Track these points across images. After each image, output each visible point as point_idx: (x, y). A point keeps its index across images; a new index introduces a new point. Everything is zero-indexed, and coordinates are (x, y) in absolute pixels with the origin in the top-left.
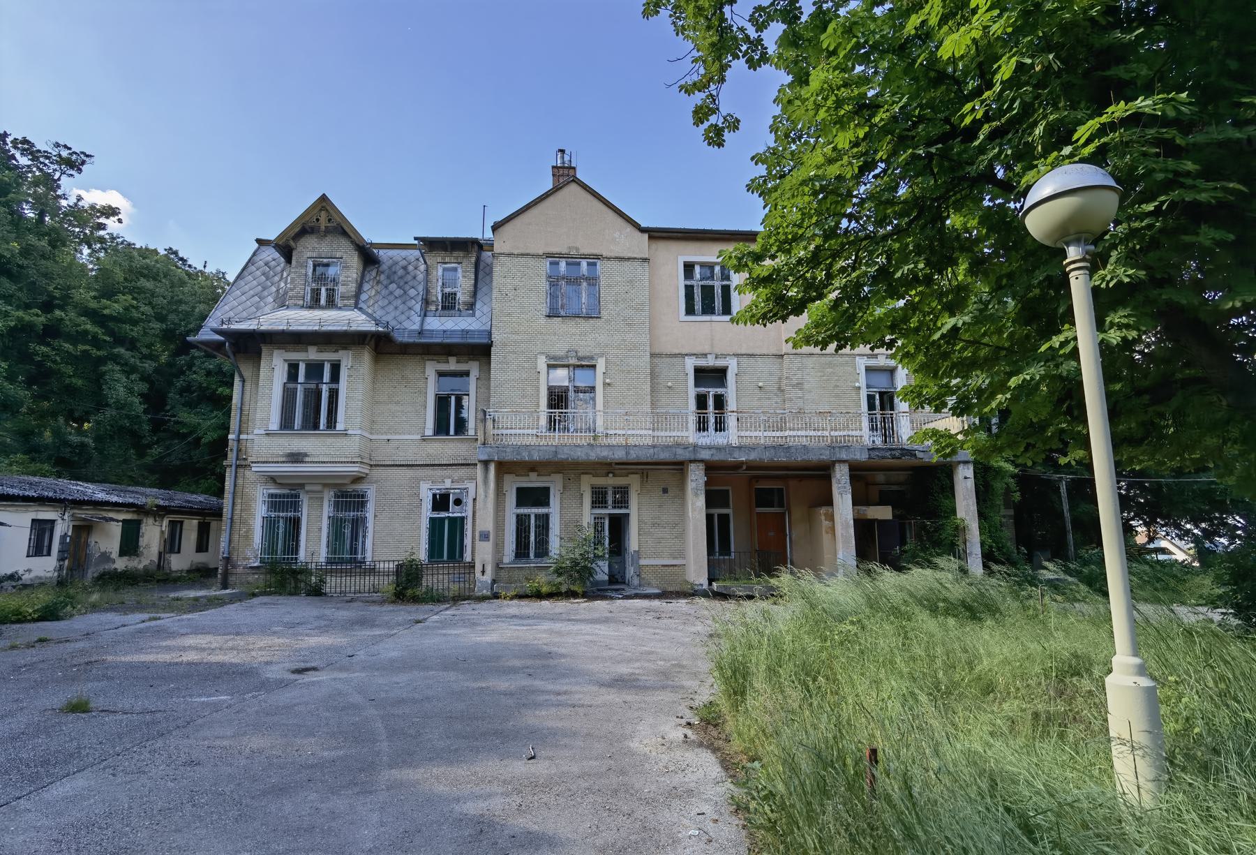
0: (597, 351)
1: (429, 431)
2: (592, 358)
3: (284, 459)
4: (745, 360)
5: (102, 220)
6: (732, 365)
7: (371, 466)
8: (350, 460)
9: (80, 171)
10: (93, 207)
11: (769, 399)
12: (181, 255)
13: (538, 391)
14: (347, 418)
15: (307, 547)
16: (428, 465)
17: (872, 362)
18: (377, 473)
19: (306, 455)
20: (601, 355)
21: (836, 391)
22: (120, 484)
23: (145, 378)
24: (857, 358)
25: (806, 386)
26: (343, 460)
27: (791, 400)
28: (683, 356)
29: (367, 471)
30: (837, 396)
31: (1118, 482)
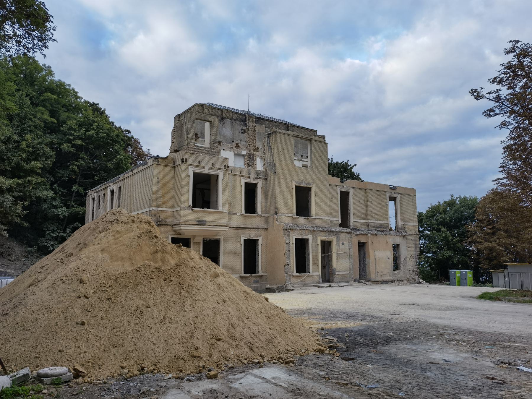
0: (312, 181)
1: (243, 212)
24: (387, 193)
26: (223, 225)
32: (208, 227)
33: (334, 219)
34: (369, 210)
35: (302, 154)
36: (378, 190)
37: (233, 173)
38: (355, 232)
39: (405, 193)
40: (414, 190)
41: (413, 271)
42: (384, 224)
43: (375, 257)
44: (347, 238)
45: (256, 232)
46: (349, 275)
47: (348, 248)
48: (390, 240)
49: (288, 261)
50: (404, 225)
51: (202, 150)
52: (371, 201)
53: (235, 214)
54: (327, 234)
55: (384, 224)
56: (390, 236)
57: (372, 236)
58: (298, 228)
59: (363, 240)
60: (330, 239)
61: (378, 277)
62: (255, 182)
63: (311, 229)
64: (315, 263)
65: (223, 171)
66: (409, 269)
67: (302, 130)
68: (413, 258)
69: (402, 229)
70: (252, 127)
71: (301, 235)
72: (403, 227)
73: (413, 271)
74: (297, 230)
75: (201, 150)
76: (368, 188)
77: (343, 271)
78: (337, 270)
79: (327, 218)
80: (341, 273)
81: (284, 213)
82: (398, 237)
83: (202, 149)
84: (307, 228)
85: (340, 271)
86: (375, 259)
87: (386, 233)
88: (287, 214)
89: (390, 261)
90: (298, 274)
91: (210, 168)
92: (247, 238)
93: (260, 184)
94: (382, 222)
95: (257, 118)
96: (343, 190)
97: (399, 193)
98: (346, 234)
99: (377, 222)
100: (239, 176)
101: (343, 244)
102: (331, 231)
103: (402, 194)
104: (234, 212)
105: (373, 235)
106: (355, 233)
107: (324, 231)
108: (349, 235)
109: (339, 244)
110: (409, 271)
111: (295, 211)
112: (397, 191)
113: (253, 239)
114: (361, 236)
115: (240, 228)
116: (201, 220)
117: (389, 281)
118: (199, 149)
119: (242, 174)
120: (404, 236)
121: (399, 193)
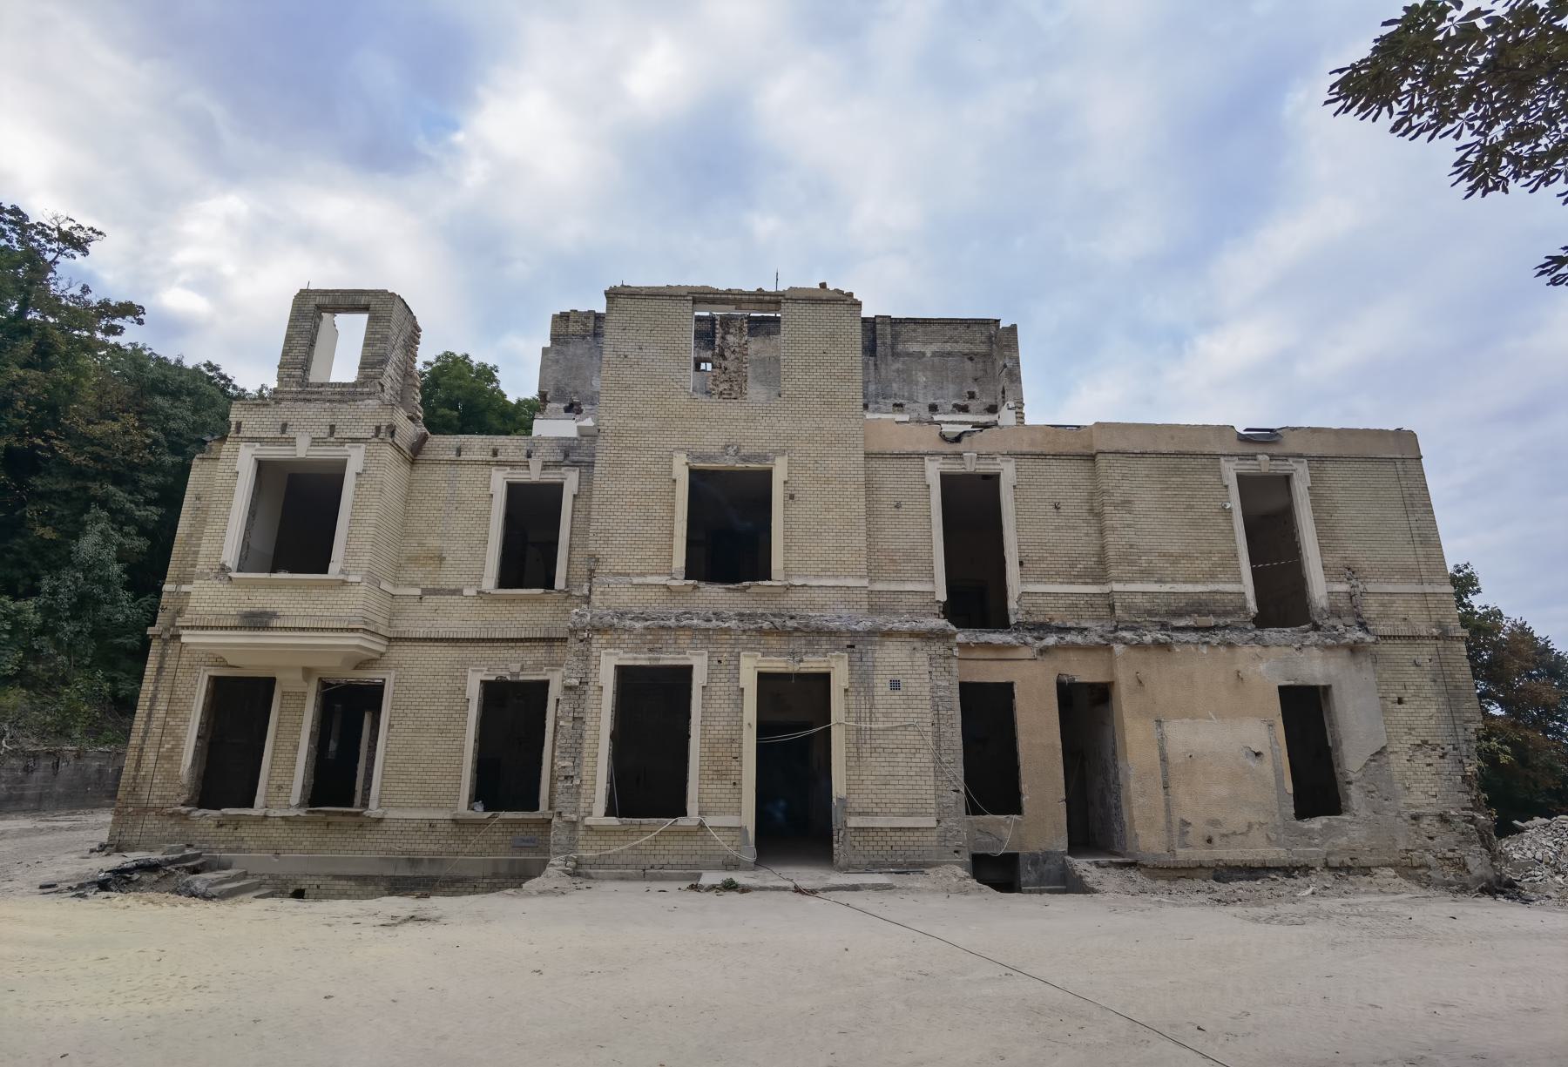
1: (489, 582)
2: (766, 458)
3: (236, 623)
4: (1028, 463)
5: (117, 322)
6: (1008, 473)
7: (390, 639)
8: (344, 625)
9: (86, 252)
10: (105, 304)
11: (1074, 528)
12: (223, 371)
13: (673, 511)
14: (349, 552)
15: (270, 777)
16: (483, 640)
17: (1248, 467)
19: (274, 615)
20: (783, 453)
23: (142, 531)
24: (1222, 459)
27: (1114, 529)
28: (921, 456)
29: (383, 649)
32: (280, 633)
33: (909, 587)
34: (1110, 538)
35: (931, 401)
36: (1164, 449)
37: (462, 458)
38: (1037, 638)
39: (1344, 453)
40: (1405, 441)
41: (1444, 819)
42: (1218, 597)
43: (1162, 749)
44: (921, 659)
45: (540, 653)
46: (932, 838)
47: (927, 705)
48: (1262, 667)
49: (566, 764)
50: (1351, 596)
51: (321, 393)
52: (1129, 502)
53: (457, 592)
54: (798, 644)
55: (1218, 597)
56: (1258, 649)
57: (1135, 655)
58: (638, 625)
59: (1085, 672)
60: (812, 664)
61: (1186, 846)
62: (551, 477)
63: (709, 625)
64: (722, 773)
65: (364, 445)
66: (1413, 811)
67: (934, 328)
68: (1439, 752)
69: (1335, 612)
70: (737, 350)
71: (650, 650)
72: (1344, 604)
73: (1444, 819)
74: (630, 630)
75: (317, 393)
76: (1104, 448)
77: (894, 814)
78: (856, 803)
79: (850, 582)
80: (880, 822)
81: (628, 575)
82: (1315, 651)
83: (320, 389)
84: (683, 623)
85: (877, 814)
86: (1164, 759)
87: (1233, 636)
88: (642, 575)
89: (1266, 767)
90: (614, 821)
91: (315, 441)
92: (493, 678)
93: (571, 481)
94: (1200, 588)
95: (1244, 439)
96: (954, 467)
97: (1300, 456)
98: (918, 644)
99: (1166, 588)
100: (488, 463)
101: (895, 685)
102: (819, 632)
103: (1321, 459)
104: (453, 587)
105: (1140, 646)
106: (1038, 644)
107: (776, 632)
108: (939, 648)
109: (869, 690)
110: (1415, 818)
111: (679, 561)
112: (1291, 445)
113: (521, 678)
114: (1073, 657)
115: (468, 640)
116: (261, 610)
117: (1268, 869)
118: (312, 393)
119: (500, 458)
120: (1354, 649)
121: (1300, 456)
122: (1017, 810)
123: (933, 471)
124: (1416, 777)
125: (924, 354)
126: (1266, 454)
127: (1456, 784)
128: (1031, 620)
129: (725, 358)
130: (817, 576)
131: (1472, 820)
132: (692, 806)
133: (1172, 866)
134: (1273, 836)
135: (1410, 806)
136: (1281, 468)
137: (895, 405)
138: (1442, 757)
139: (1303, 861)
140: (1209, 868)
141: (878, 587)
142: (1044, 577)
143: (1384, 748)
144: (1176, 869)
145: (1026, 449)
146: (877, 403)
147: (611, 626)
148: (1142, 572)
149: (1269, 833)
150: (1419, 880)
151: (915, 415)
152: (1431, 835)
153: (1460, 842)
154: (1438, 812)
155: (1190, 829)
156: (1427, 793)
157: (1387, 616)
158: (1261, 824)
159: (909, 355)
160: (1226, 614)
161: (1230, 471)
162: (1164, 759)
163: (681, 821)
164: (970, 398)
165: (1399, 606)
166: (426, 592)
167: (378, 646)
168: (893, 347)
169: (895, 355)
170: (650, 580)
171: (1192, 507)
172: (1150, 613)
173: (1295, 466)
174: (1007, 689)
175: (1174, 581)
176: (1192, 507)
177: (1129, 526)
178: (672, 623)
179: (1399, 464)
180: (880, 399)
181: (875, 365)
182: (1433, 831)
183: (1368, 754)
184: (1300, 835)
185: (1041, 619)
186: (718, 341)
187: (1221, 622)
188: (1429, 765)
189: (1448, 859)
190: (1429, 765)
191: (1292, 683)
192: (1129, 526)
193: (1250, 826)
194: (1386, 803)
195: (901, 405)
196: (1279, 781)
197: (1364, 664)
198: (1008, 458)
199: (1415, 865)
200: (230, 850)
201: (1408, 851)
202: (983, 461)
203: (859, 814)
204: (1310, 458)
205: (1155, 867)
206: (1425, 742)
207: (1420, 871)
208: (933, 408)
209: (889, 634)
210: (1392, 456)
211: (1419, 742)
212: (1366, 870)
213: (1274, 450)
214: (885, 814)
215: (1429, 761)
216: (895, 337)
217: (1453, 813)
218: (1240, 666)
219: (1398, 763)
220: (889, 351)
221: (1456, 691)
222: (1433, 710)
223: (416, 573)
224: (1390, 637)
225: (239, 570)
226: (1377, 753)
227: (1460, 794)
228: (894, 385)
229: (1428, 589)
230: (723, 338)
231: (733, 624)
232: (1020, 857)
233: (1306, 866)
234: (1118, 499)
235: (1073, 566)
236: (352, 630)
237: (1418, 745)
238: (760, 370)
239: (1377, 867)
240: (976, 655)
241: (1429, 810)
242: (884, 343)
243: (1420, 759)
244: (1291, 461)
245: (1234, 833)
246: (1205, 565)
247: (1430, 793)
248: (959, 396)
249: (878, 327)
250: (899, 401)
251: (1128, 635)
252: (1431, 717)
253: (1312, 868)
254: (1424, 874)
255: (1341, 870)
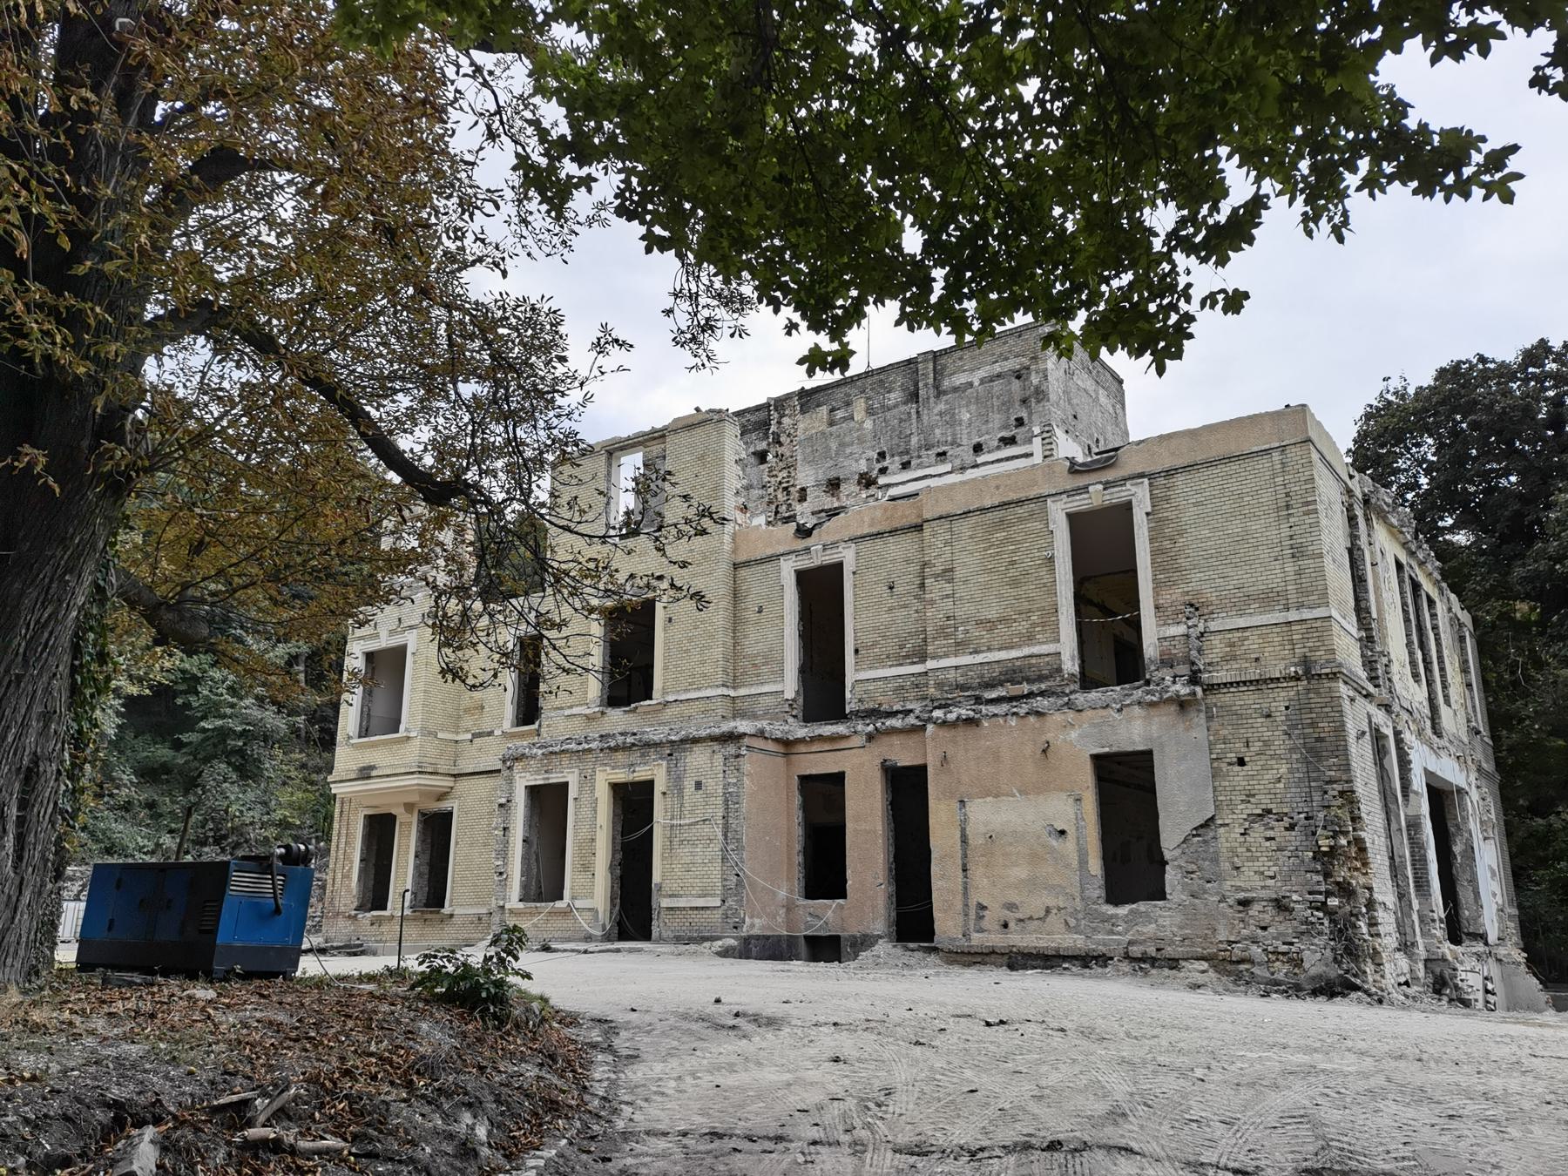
1: (507, 724)
4: (867, 545)
7: (454, 776)
11: (905, 606)
17: (1079, 504)
18: (463, 785)
19: (372, 768)
21: (1012, 572)
22: (332, 817)
25: (958, 574)
26: (403, 771)
29: (451, 784)
30: (1015, 583)
31: (1486, 698)
33: (765, 689)
35: (976, 440)
36: (988, 503)
39: (1199, 458)
41: (1281, 906)
42: (1033, 661)
43: (963, 831)
44: (719, 758)
46: (718, 915)
47: (720, 801)
48: (1074, 735)
53: (490, 734)
54: (635, 756)
55: (1033, 661)
56: (1071, 715)
57: (945, 734)
59: (904, 756)
60: (641, 774)
61: (981, 931)
63: (580, 748)
64: (586, 867)
66: (1241, 895)
73: (1281, 906)
74: (533, 757)
76: (927, 516)
77: (693, 896)
78: (666, 889)
80: (681, 903)
81: (562, 708)
85: (681, 896)
86: (964, 840)
87: (1041, 703)
88: (571, 707)
89: (1069, 846)
90: (521, 905)
94: (1014, 654)
96: (805, 563)
98: (716, 747)
99: (979, 658)
101: (698, 785)
102: (649, 745)
103: (1169, 473)
109: (681, 791)
110: (1245, 903)
112: (1131, 463)
114: (896, 740)
117: (1066, 958)
122: (843, 896)
123: (787, 570)
124: (1249, 854)
125: (971, 384)
126: (1100, 483)
127: (1303, 861)
128: (862, 708)
129: (781, 444)
130: (686, 691)
131: (1323, 907)
132: (567, 893)
133: (966, 950)
134: (1072, 922)
135: (1239, 889)
136: (1116, 496)
137: (939, 455)
138: (1291, 827)
139: (1101, 949)
140: (1003, 954)
141: (742, 692)
142: (880, 662)
143: (1212, 819)
144: (969, 953)
145: (866, 531)
146: (919, 457)
147: (523, 755)
148: (958, 644)
149: (1069, 919)
150: (1238, 977)
151: (958, 462)
152: (1263, 924)
153: (1302, 933)
154: (1274, 896)
155: (986, 913)
156: (1262, 873)
157: (1234, 658)
158: (1059, 909)
159: (955, 389)
160: (1041, 678)
161: (1058, 514)
162: (964, 840)
163: (559, 904)
164: (1016, 427)
165: (1253, 643)
166: (475, 736)
167: (447, 782)
168: (937, 387)
169: (940, 393)
170: (575, 710)
171: (1013, 563)
172: (963, 688)
173: (1134, 489)
174: (838, 779)
175: (989, 649)
176: (1013, 563)
177: (947, 596)
178: (556, 749)
179: (1276, 456)
180: (923, 452)
181: (918, 412)
182: (1267, 918)
183: (1188, 828)
184: (1103, 921)
185: (871, 705)
186: (773, 428)
187: (1035, 688)
188: (1268, 839)
189: (1284, 954)
190: (1268, 839)
191: (1107, 750)
192: (947, 596)
193: (1048, 911)
194: (1209, 885)
195: (944, 454)
196: (1083, 862)
197: (1196, 720)
198: (850, 544)
199: (1234, 959)
200: (377, 942)
201: (1230, 943)
202: (828, 552)
203: (670, 896)
204: (1151, 476)
205: (950, 952)
206: (1269, 811)
207: (1242, 967)
208: (978, 448)
209: (696, 741)
210: (1267, 447)
211: (1260, 811)
212: (1174, 963)
213: (1110, 475)
214: (687, 896)
215: (1270, 834)
216: (938, 374)
217: (1295, 897)
218: (1049, 736)
219: (1228, 838)
220: (932, 392)
221: (1318, 745)
222: (1283, 770)
223: (468, 722)
224: (1231, 684)
225: (360, 737)
226: (1202, 826)
227: (1308, 875)
228: (937, 431)
229: (1293, 616)
230: (779, 423)
231: (593, 745)
232: (843, 943)
233: (1104, 955)
234: (939, 569)
235: (902, 647)
236: (412, 773)
237: (1259, 815)
238: (809, 450)
239: (1186, 960)
240: (814, 748)
241: (1264, 894)
242: (926, 385)
243: (1258, 831)
244: (1128, 483)
245: (1031, 918)
246: (1022, 627)
247: (1267, 873)
248: (1005, 427)
249: (920, 366)
250: (940, 450)
251: (938, 713)
252: (1279, 781)
253: (1112, 958)
254: (1247, 970)
255: (1145, 962)
